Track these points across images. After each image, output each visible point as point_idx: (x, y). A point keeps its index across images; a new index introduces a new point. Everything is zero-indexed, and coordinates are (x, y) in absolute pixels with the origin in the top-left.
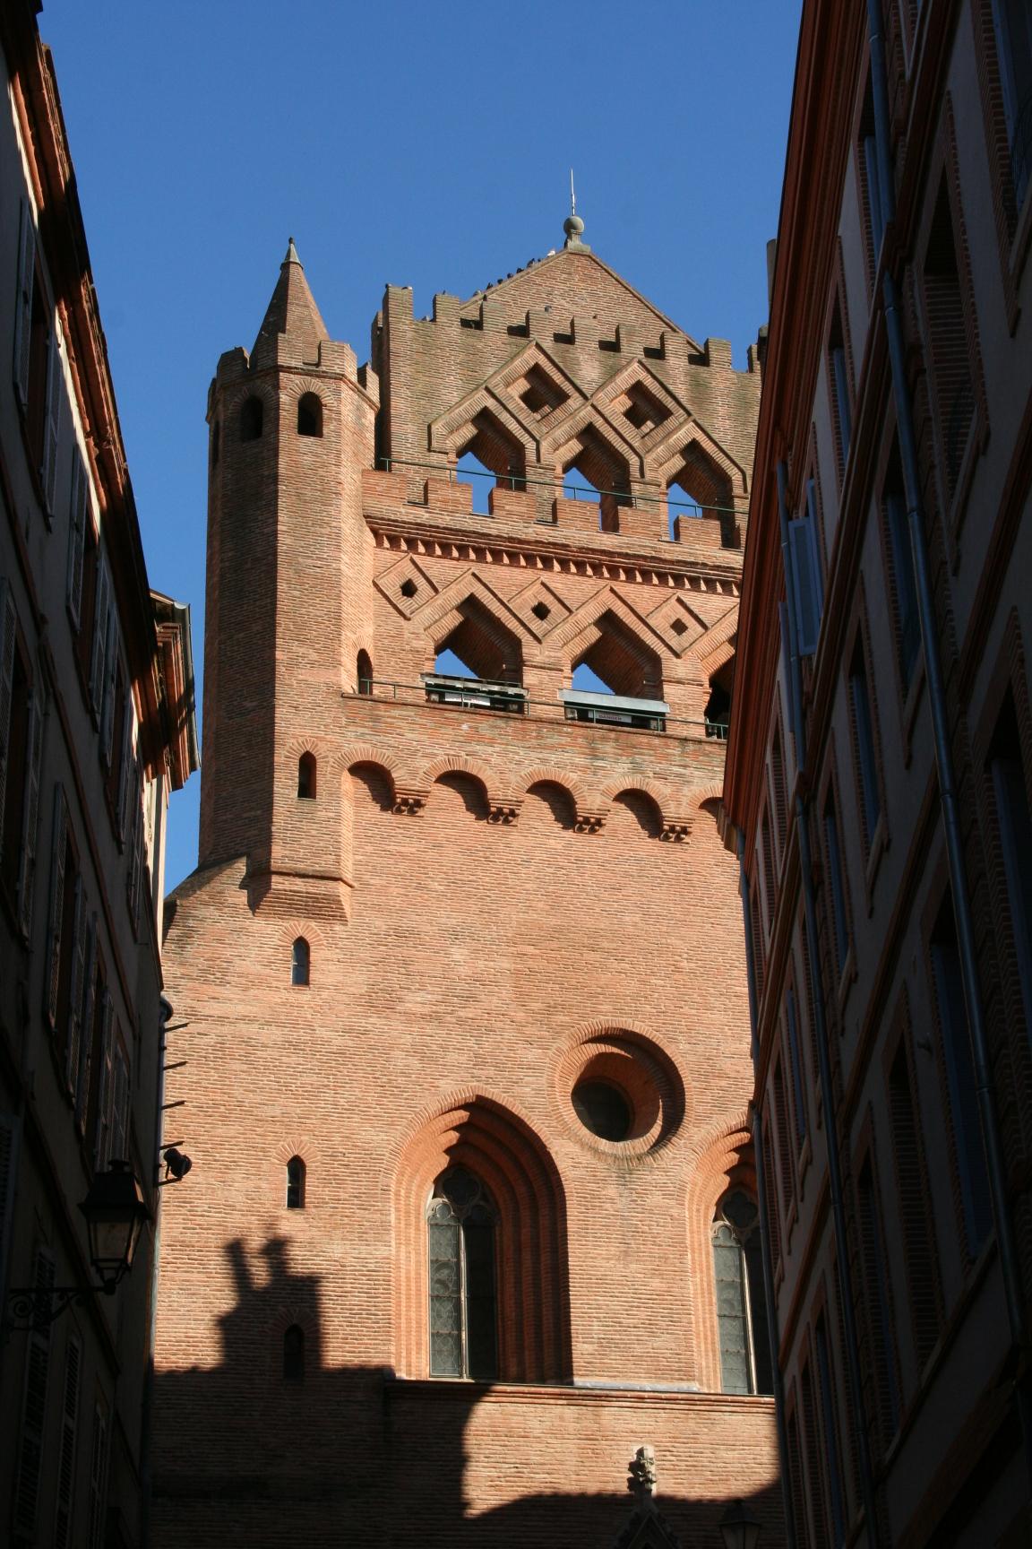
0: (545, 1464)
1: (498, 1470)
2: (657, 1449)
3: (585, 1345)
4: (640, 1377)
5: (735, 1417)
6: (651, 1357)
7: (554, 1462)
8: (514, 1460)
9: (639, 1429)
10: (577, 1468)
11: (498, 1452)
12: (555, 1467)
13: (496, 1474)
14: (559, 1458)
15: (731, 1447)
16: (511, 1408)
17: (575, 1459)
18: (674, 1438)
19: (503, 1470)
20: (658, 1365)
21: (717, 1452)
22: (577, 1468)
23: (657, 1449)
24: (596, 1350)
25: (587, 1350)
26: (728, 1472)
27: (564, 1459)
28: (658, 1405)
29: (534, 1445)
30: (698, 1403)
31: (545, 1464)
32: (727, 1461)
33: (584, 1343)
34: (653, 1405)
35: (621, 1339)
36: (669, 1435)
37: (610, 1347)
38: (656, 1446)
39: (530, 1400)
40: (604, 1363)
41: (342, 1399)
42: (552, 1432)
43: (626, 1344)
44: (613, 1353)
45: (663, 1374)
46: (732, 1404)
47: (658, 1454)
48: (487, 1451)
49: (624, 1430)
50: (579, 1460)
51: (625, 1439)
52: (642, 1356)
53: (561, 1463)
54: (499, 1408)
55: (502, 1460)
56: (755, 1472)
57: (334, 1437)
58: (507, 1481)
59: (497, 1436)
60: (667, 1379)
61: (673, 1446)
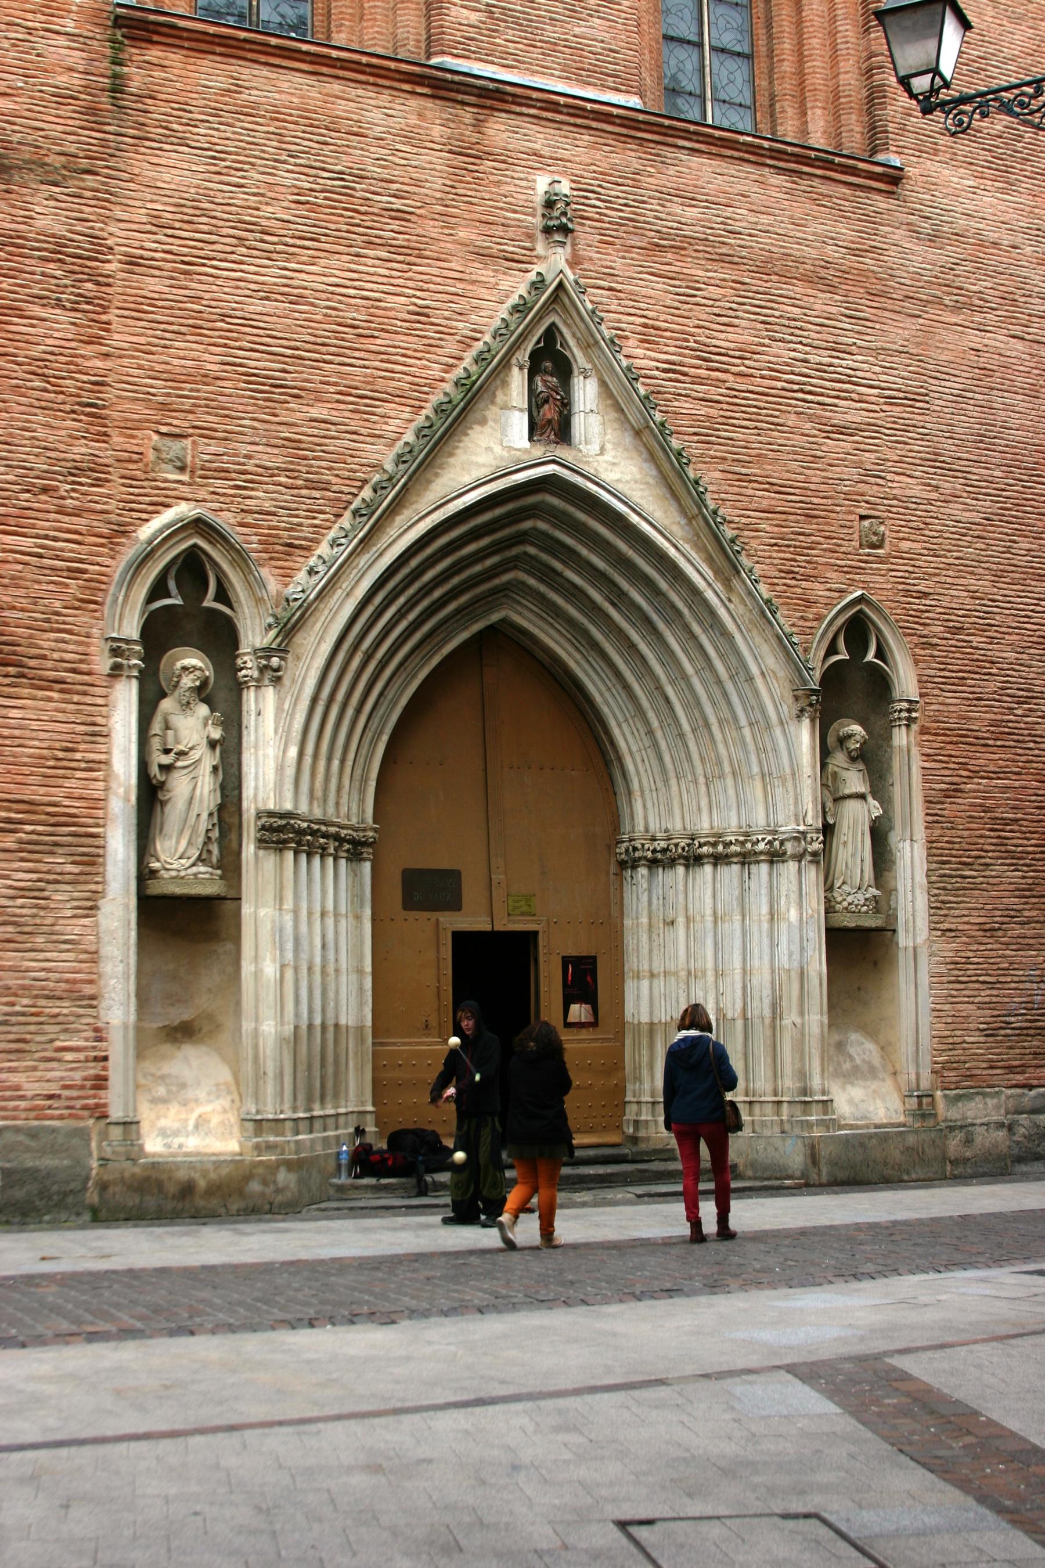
0: (392, 182)
1: (311, 179)
2: (574, 185)
3: (465, 11)
4: (552, 75)
5: (696, 160)
6: (570, 47)
7: (407, 180)
8: (338, 168)
9: (546, 151)
10: (443, 195)
11: (313, 151)
12: (406, 188)
13: (309, 186)
14: (414, 175)
15: (691, 201)
16: (336, 87)
17: (440, 181)
18: (602, 173)
19: (319, 180)
20: (581, 62)
21: (668, 204)
22: (443, 195)
23: (574, 185)
24: (484, 23)
25: (467, 18)
26: (685, 236)
27: (423, 177)
28: (579, 121)
29: (373, 149)
30: (642, 126)
31: (392, 182)
32: (683, 220)
33: (462, 7)
34: (572, 120)
35: (524, 13)
36: (594, 168)
37: (506, 21)
38: (573, 181)
39: (371, 79)
40: (494, 44)
41: (38, 25)
42: (407, 136)
43: (531, 21)
44: (511, 32)
45: (588, 76)
46: (695, 138)
47: (575, 193)
48: (293, 147)
49: (522, 149)
50: (449, 183)
51: (523, 163)
52: (555, 44)
53: (418, 183)
54: (316, 83)
55: (317, 164)
56: (723, 243)
57: (21, 84)
58: (326, 199)
59: (311, 126)
60: (595, 85)
61: (600, 186)
